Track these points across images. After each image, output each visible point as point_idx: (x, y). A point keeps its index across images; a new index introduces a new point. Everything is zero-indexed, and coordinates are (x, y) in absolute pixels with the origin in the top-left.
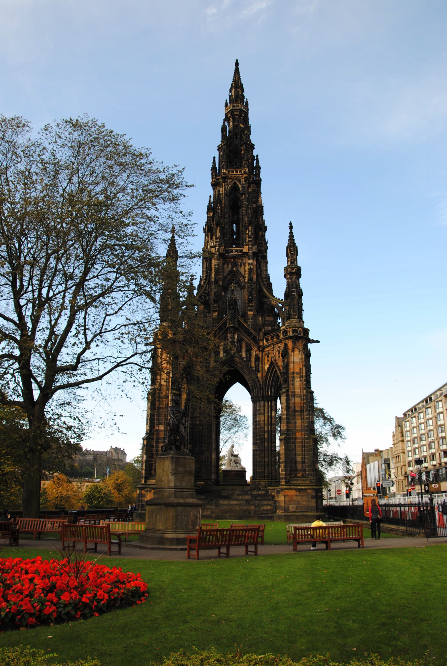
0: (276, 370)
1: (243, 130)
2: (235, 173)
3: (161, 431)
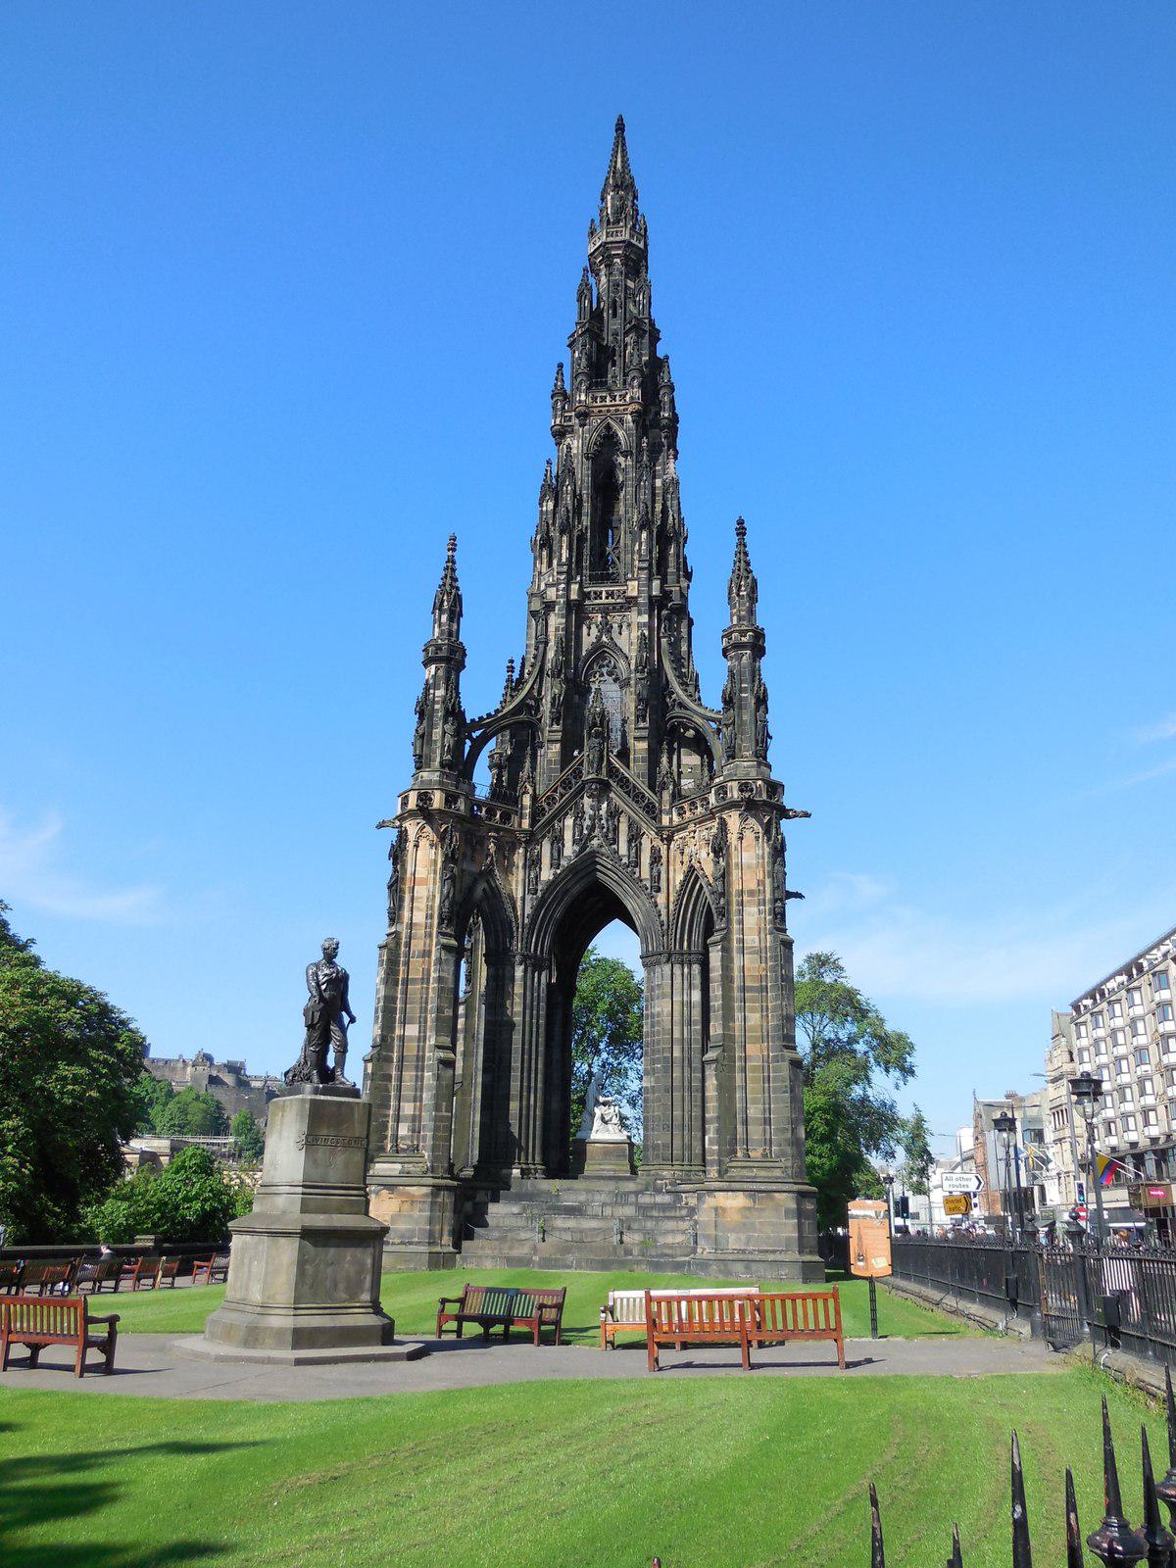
0: (701, 887)
1: (630, 295)
2: (608, 398)
3: (411, 1038)
